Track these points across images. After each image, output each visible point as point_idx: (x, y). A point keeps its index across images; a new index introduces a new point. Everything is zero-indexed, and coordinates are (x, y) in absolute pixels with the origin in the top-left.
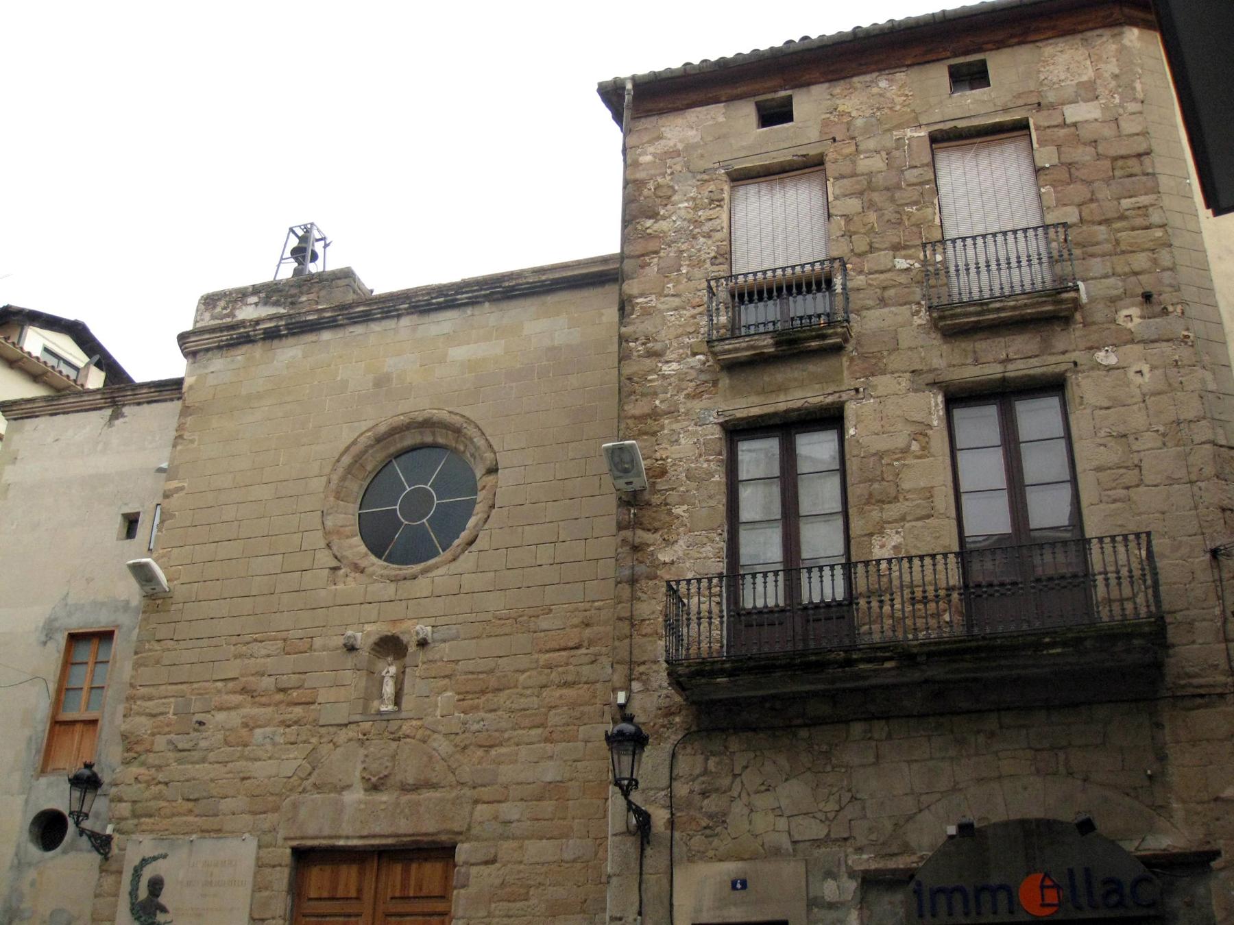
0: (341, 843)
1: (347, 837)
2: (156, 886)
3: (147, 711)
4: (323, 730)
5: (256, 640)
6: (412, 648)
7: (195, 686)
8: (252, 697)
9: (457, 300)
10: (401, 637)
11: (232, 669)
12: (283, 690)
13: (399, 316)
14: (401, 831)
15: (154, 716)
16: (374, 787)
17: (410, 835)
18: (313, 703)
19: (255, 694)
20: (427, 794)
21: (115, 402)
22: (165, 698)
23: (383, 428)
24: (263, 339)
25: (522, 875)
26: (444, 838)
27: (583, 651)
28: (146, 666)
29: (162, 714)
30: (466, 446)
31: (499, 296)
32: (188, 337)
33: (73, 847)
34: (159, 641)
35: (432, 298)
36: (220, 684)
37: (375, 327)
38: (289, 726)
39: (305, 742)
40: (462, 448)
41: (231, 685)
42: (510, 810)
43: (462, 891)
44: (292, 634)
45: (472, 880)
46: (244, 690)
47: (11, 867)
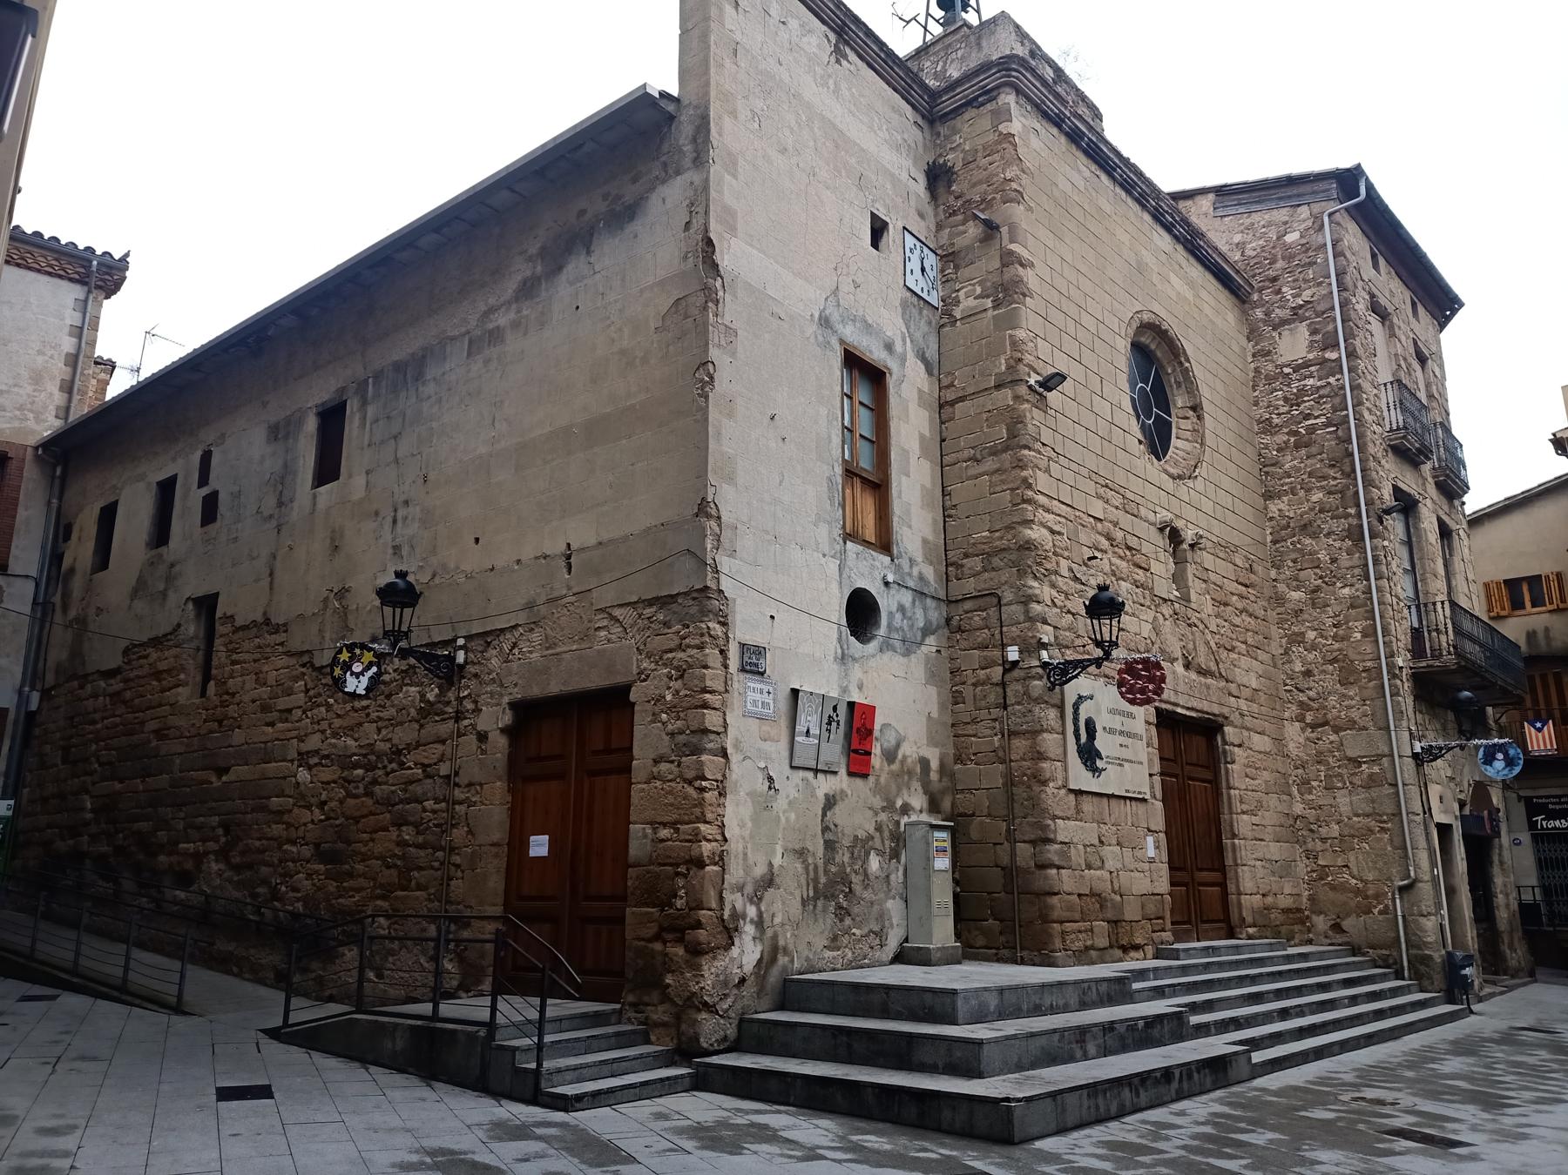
0: (1179, 710)
1: (1183, 707)
2: (1090, 726)
3: (1049, 524)
4: (1155, 598)
5: (1107, 486)
6: (1185, 546)
7: (1077, 513)
8: (1112, 545)
9: (1175, 227)
10: (1182, 533)
11: (1097, 509)
12: (1129, 548)
13: (1143, 207)
14: (1205, 709)
15: (1053, 532)
16: (1187, 666)
17: (1208, 713)
18: (1148, 570)
19: (1114, 544)
20: (1209, 681)
21: (842, 29)
22: (1059, 515)
23: (1146, 317)
24: (1067, 135)
25: (1253, 759)
26: (1220, 719)
27: (1250, 590)
28: (1040, 470)
29: (1059, 533)
30: (1174, 371)
31: (1189, 246)
32: (1026, 69)
33: (886, 646)
34: (1044, 444)
35: (1167, 212)
36: (1092, 520)
37: (1129, 201)
38: (1137, 587)
39: (1149, 607)
40: (1170, 371)
41: (1099, 525)
42: (1243, 705)
43: (1234, 766)
44: (1129, 495)
45: (1237, 758)
46: (1109, 538)
47: (836, 658)
